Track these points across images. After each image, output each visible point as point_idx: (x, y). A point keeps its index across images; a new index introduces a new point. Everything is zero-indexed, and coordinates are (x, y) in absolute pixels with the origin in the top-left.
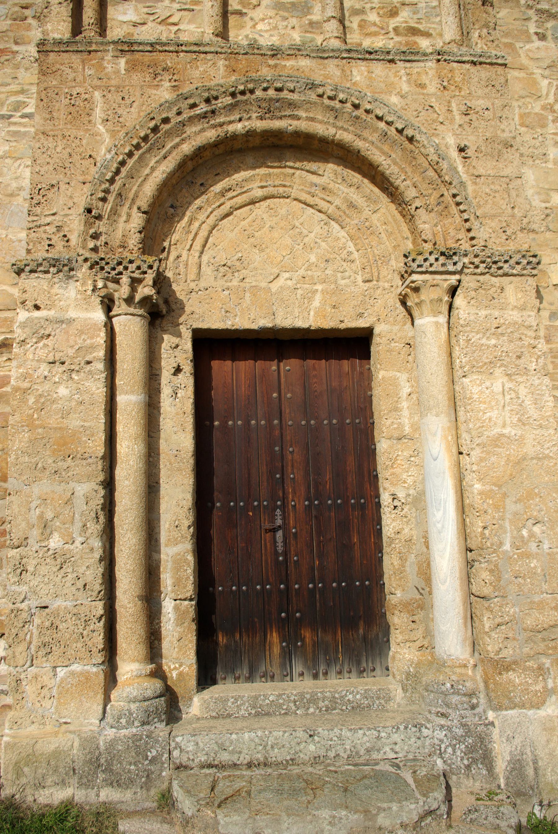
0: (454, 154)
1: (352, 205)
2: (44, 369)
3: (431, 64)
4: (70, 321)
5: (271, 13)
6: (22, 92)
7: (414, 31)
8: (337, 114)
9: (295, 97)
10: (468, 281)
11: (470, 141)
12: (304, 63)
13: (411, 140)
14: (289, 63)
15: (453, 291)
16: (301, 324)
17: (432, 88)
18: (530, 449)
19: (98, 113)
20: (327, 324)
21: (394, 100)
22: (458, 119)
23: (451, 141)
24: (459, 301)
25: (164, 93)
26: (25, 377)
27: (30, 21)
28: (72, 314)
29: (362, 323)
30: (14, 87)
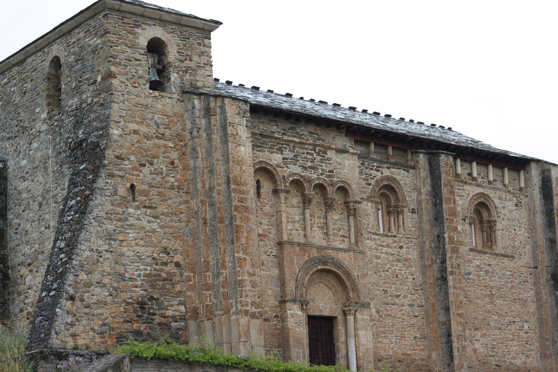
0: (356, 277)
1: (334, 285)
2: (294, 325)
3: (352, 253)
4: (297, 314)
5: (317, 229)
6: (272, 248)
7: (344, 236)
8: (335, 265)
9: (329, 261)
10: (359, 309)
11: (359, 274)
12: (330, 251)
13: (350, 274)
14: (328, 251)
15: (356, 311)
16: (325, 315)
17: (353, 260)
19: (295, 262)
20: (330, 315)
21: (346, 263)
23: (356, 274)
24: (357, 313)
25: (307, 258)
26: (291, 326)
27: (270, 227)
28: (296, 312)
29: (335, 315)
30: (270, 247)
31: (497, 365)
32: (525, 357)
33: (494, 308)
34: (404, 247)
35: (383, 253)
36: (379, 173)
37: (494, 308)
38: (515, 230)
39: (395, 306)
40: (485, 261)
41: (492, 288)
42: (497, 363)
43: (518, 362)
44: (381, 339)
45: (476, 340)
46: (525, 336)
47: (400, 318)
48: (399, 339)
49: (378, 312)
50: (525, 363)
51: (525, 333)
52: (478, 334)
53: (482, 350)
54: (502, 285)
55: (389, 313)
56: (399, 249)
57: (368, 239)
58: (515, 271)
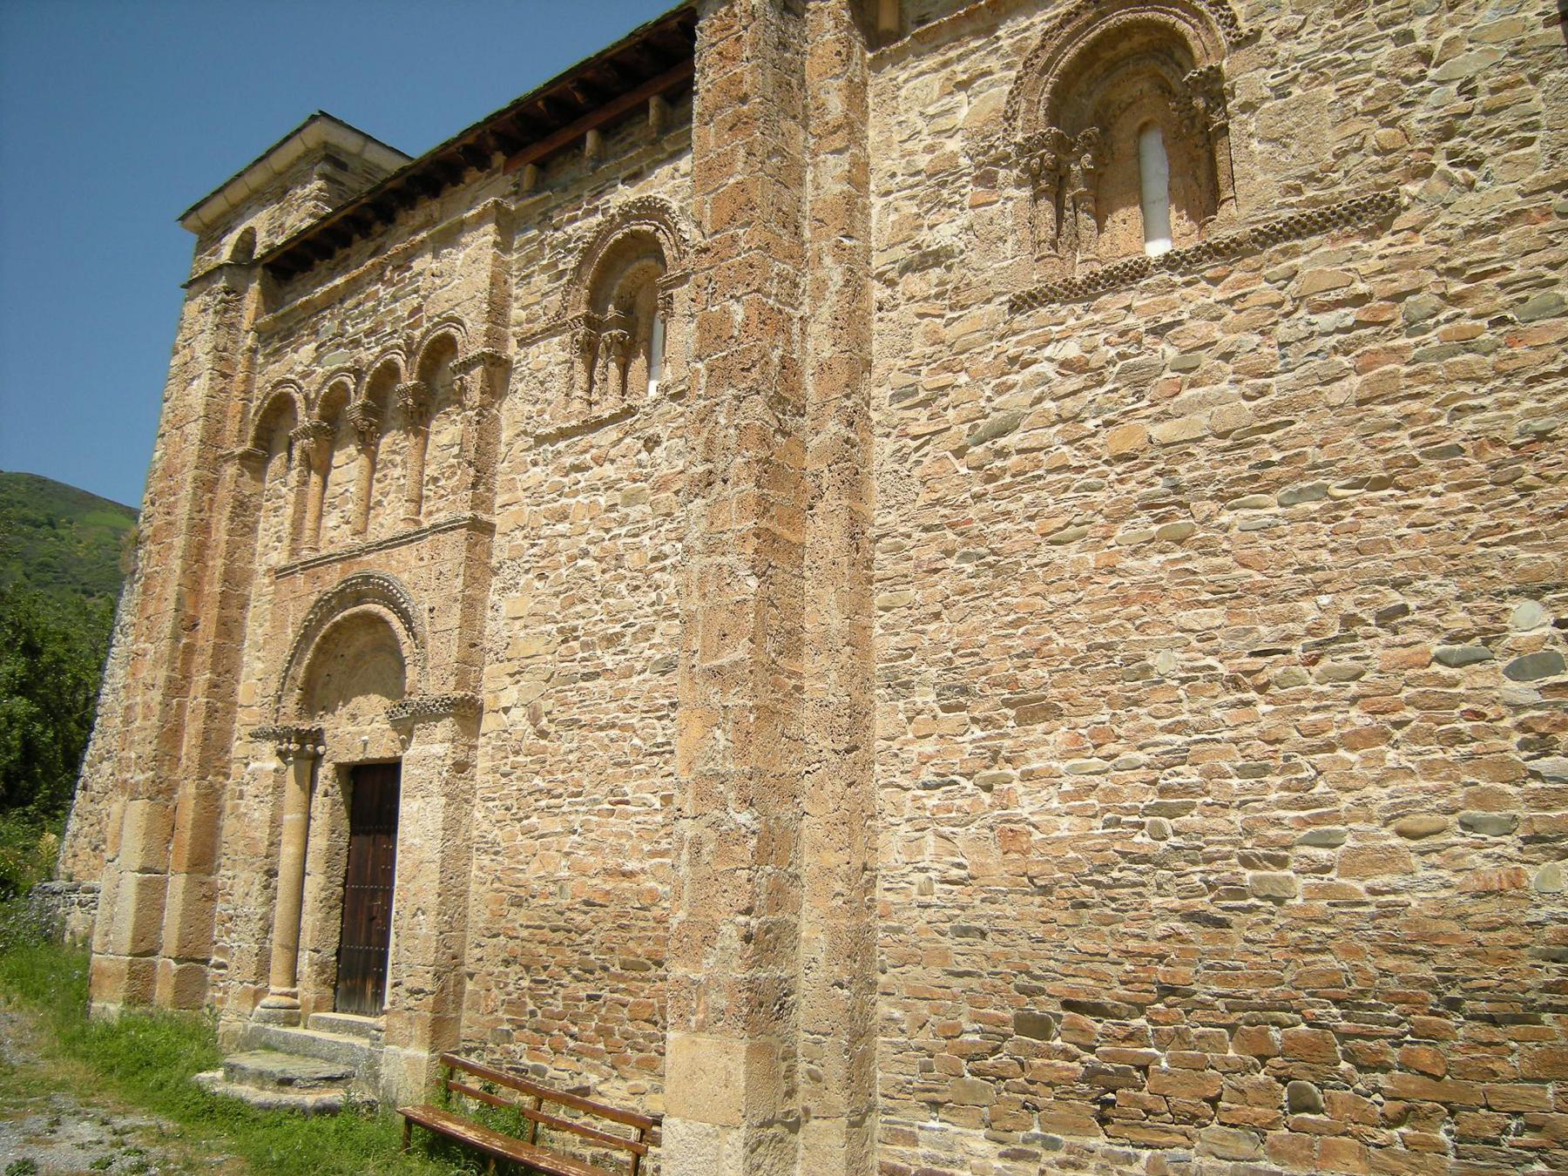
18: (426, 856)
22: (434, 583)
31: (1192, 917)
32: (1511, 845)
33: (1199, 564)
34: (664, 436)
35: (576, 494)
36: (599, 217)
37: (1199, 564)
38: (1408, 36)
39: (600, 680)
40: (1131, 320)
41: (1180, 449)
42: (1202, 904)
43: (1424, 888)
44: (534, 819)
45: (1028, 776)
46: (1523, 691)
47: (613, 726)
48: (599, 813)
49: (534, 718)
50: (1508, 890)
51: (1515, 672)
52: (1046, 744)
53: (1065, 827)
54: (1275, 409)
55: (574, 712)
56: (644, 455)
57: (535, 464)
58: (1403, 281)
